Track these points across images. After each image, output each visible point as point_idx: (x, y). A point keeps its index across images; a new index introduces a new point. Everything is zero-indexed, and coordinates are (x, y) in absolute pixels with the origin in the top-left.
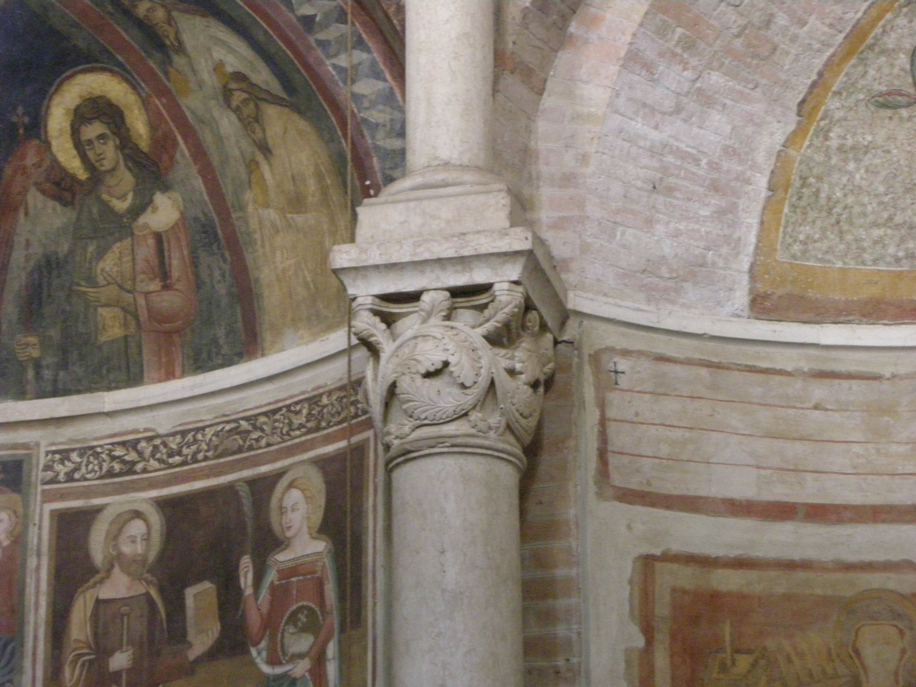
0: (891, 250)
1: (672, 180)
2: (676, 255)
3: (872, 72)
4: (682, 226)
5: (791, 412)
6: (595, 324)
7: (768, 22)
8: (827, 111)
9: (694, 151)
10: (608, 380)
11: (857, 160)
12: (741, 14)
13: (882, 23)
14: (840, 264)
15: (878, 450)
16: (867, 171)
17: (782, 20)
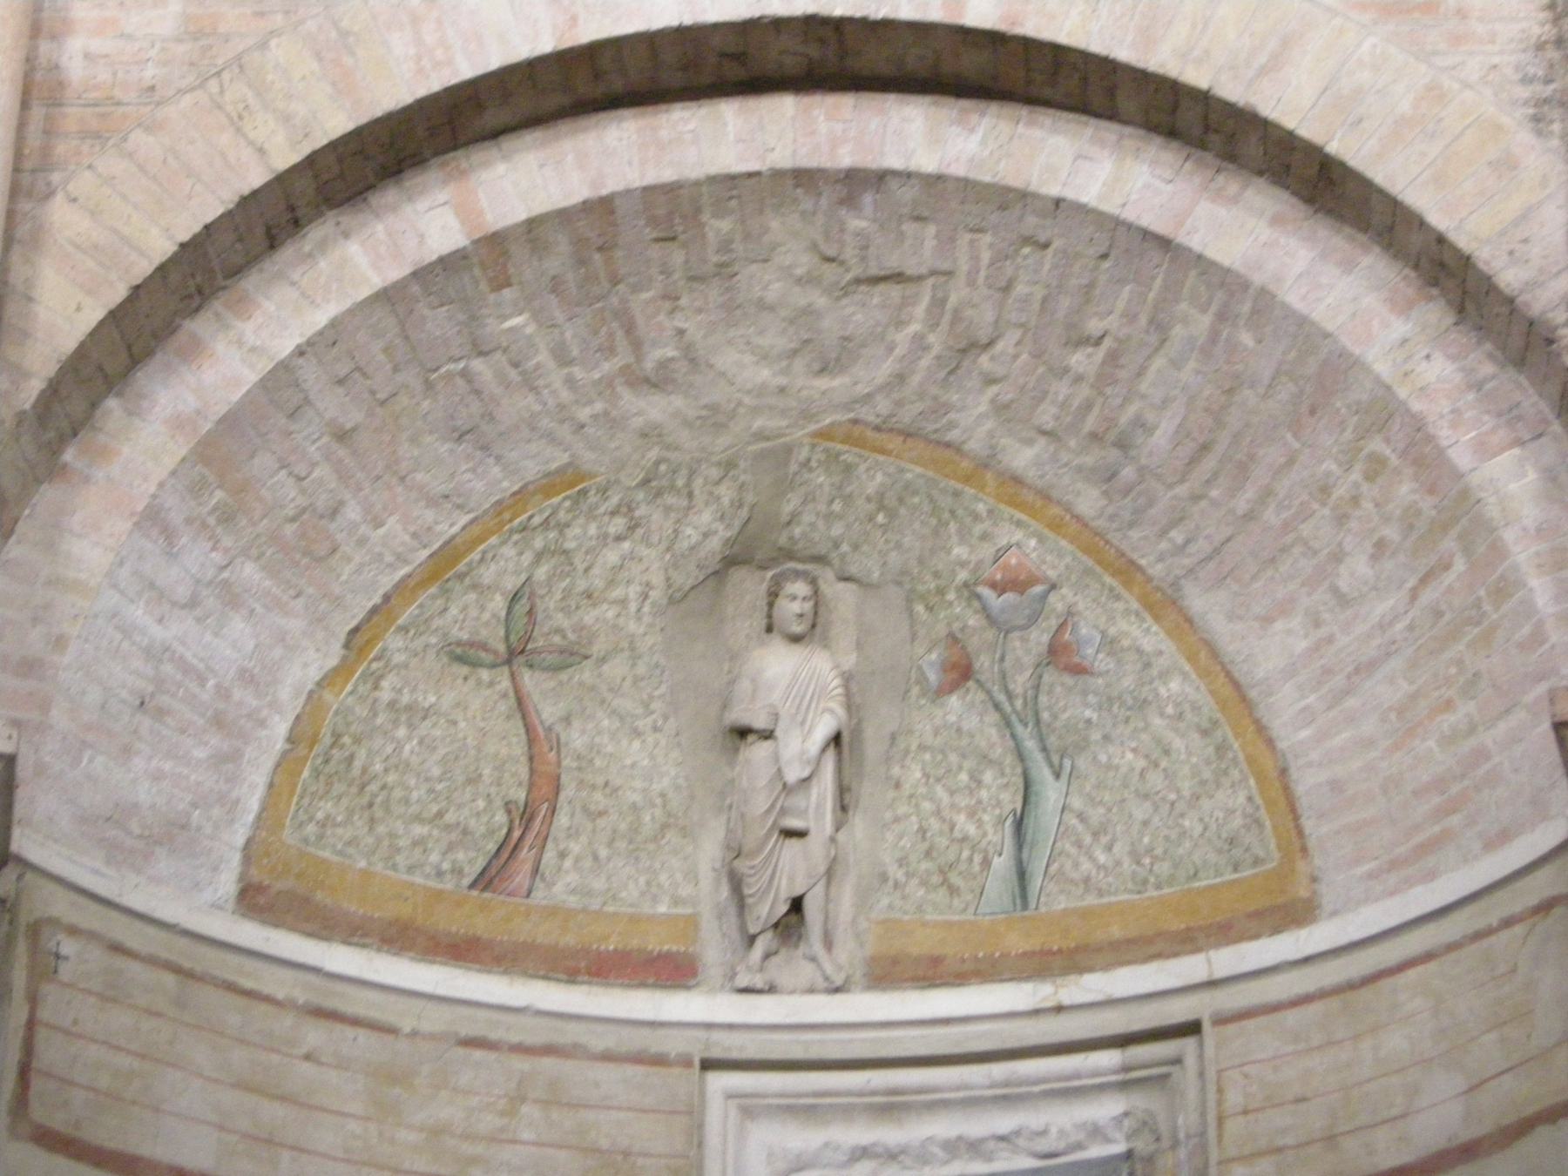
0: (434, 857)
1: (164, 700)
2: (153, 806)
3: (454, 611)
4: (168, 766)
5: (275, 1058)
6: (43, 882)
7: (334, 512)
8: (384, 650)
9: (201, 666)
10: (45, 967)
11: (411, 726)
12: (303, 491)
13: (482, 547)
14: (362, 864)
15: (381, 1134)
16: (421, 742)
17: (352, 512)
